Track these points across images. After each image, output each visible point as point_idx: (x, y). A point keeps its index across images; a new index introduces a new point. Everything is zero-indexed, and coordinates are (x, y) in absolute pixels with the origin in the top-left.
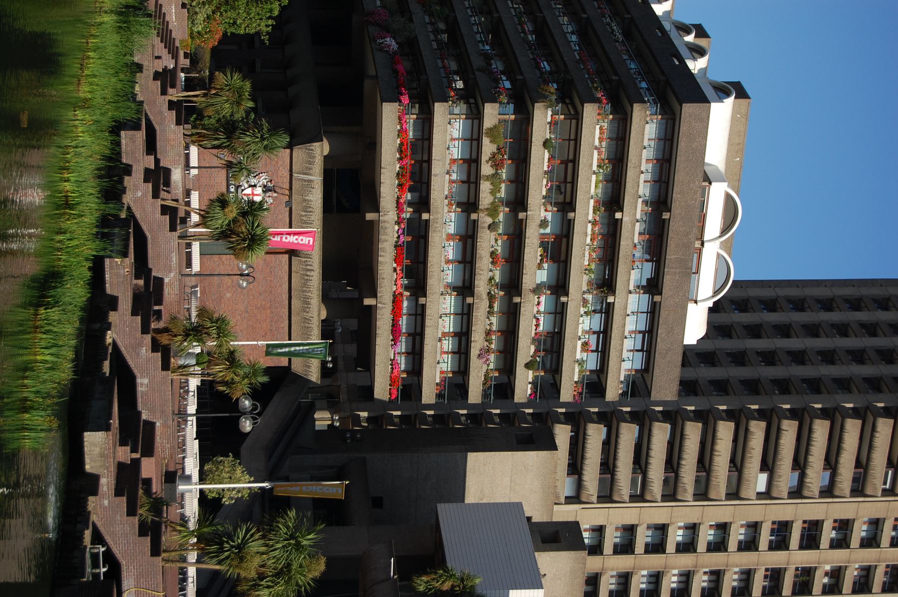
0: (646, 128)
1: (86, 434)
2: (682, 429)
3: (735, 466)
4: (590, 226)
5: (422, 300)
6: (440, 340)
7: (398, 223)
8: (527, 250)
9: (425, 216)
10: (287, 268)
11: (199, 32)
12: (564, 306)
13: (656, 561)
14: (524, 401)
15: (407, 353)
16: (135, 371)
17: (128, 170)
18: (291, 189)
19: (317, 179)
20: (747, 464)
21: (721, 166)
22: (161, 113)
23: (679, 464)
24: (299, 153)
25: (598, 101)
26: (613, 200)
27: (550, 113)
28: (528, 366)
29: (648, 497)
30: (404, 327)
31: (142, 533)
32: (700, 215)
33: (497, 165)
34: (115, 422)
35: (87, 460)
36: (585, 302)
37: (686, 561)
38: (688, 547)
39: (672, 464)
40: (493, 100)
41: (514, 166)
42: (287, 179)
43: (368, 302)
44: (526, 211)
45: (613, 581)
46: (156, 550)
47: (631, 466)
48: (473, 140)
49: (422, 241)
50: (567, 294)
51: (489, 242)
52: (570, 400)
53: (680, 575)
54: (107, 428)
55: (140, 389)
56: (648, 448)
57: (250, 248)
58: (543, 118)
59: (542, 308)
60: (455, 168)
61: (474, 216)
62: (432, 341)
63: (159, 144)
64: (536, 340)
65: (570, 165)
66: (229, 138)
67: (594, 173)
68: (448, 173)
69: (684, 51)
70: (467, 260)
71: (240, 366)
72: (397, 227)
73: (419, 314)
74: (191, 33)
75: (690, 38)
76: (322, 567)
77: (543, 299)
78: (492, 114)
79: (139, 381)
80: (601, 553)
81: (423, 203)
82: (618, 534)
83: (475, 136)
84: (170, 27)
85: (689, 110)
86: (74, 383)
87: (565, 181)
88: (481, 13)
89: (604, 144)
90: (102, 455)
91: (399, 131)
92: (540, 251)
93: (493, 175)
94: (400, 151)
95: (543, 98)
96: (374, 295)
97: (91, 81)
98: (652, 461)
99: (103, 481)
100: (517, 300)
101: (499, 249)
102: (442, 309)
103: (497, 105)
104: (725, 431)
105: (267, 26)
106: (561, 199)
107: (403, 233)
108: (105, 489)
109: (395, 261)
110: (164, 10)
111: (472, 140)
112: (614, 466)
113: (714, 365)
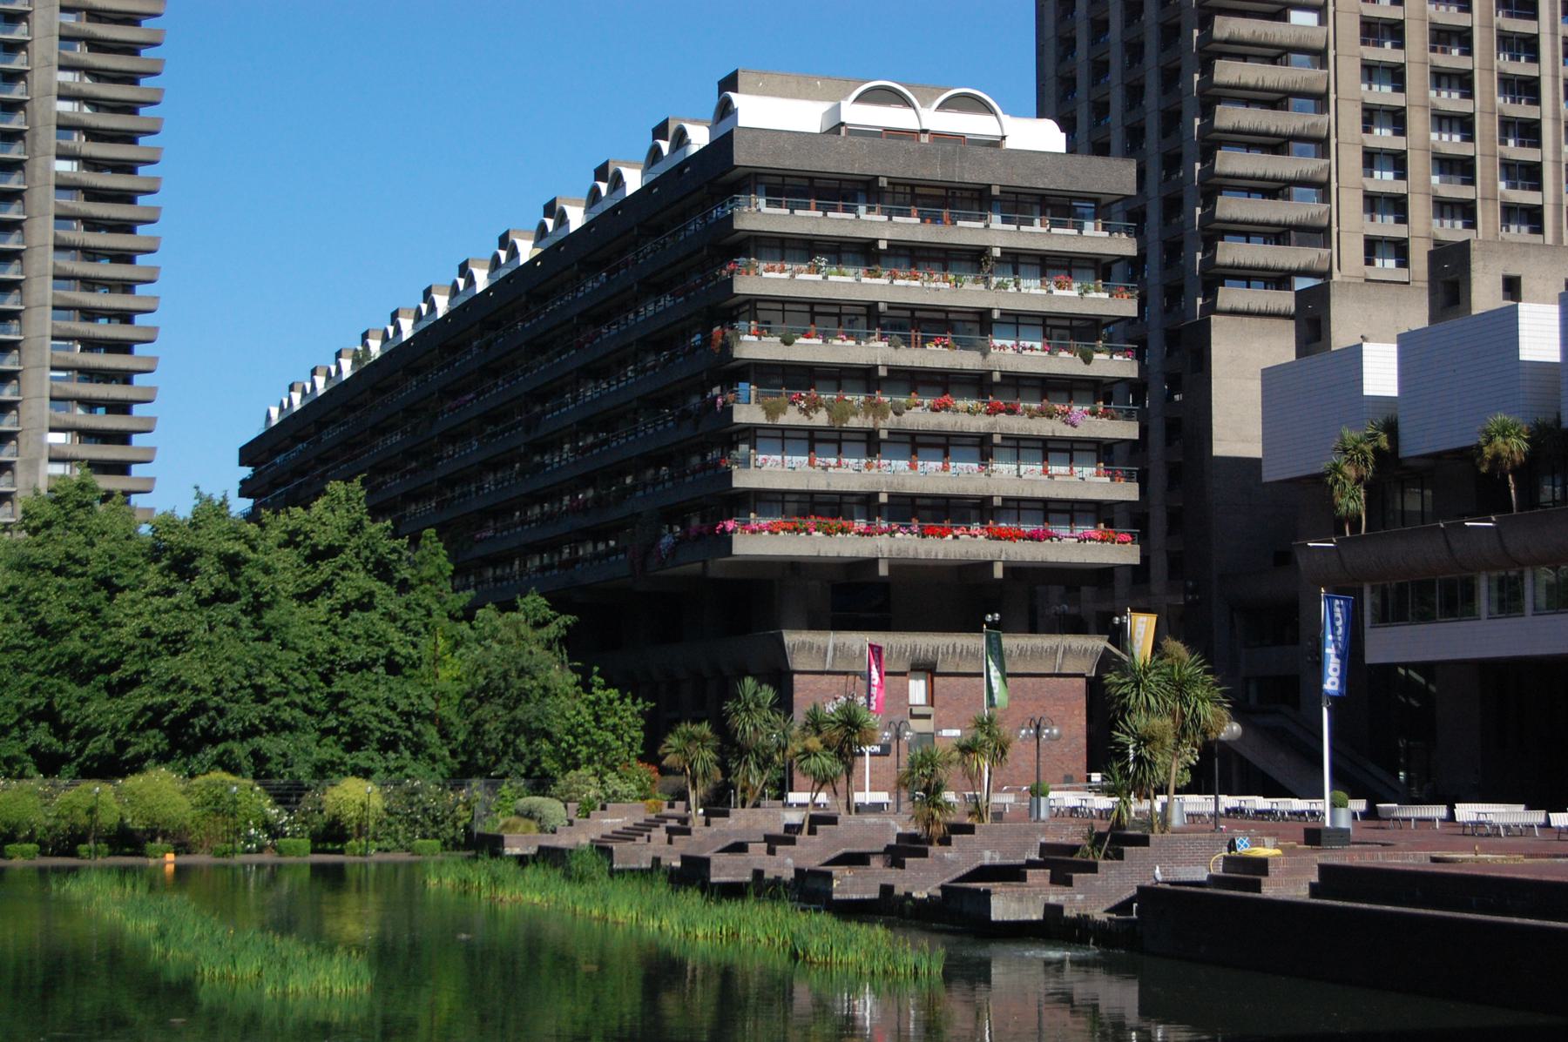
0: (759, 215)
1: (993, 918)
2: (1226, 131)
3: (1280, 56)
4: (896, 282)
5: (997, 502)
6: (1051, 477)
7: (892, 533)
8: (929, 364)
9: (883, 498)
10: (952, 679)
11: (640, 790)
12: (1004, 313)
13: (1418, 164)
14: (1135, 365)
15: (1072, 522)
16: (975, 865)
17: (887, 890)
18: (846, 673)
19: (831, 639)
20: (1277, 40)
21: (825, 106)
22: (712, 836)
23: (1276, 135)
24: (798, 662)
25: (732, 273)
26: (865, 253)
27: (746, 338)
28: (1087, 360)
29: (1324, 177)
30: (1035, 527)
31: (1119, 856)
32: (888, 137)
33: (814, 406)
34: (981, 886)
35: (1026, 917)
36: (998, 286)
37: (1418, 121)
38: (1397, 120)
39: (1277, 144)
40: (728, 411)
41: (818, 383)
42: (835, 678)
43: (998, 573)
44: (876, 367)
45: (1447, 223)
46: (1143, 841)
47: (1280, 201)
48: (785, 438)
49: (919, 502)
50: (990, 310)
51: (920, 415)
52: (1135, 303)
53: (1440, 129)
54: (987, 893)
55: (998, 860)
56: (1253, 178)
57: (857, 727)
58: (753, 346)
59: (1009, 343)
60: (818, 461)
61: (883, 435)
62: (1058, 489)
63: (862, 849)
64: (1050, 350)
65: (817, 309)
66: (749, 751)
67: (825, 278)
68: (825, 468)
69: (679, 158)
70: (944, 444)
71: (975, 739)
72: (899, 535)
73: (1017, 506)
74: (643, 799)
75: (665, 146)
76: (1178, 644)
77: (997, 342)
78: (748, 413)
79: (987, 862)
80: (1406, 240)
81: (867, 504)
82: (1378, 217)
83: (779, 433)
84: (630, 825)
85: (742, 156)
86: (888, 925)
87: (839, 315)
88: (636, 421)
89: (788, 266)
90: (1020, 900)
91: (771, 532)
92: (930, 347)
93: (828, 409)
94: (798, 530)
95: (727, 347)
96: (989, 565)
97: (691, 927)
98: (1270, 173)
99: (1052, 900)
100: (997, 377)
101: (927, 402)
102: (1009, 477)
103: (736, 407)
104: (1228, 72)
105: (634, 703)
106: (863, 320)
107: (907, 527)
108: (1062, 898)
109: (942, 536)
110: (609, 833)
111: (783, 438)
112: (1278, 225)
113: (1142, 87)
